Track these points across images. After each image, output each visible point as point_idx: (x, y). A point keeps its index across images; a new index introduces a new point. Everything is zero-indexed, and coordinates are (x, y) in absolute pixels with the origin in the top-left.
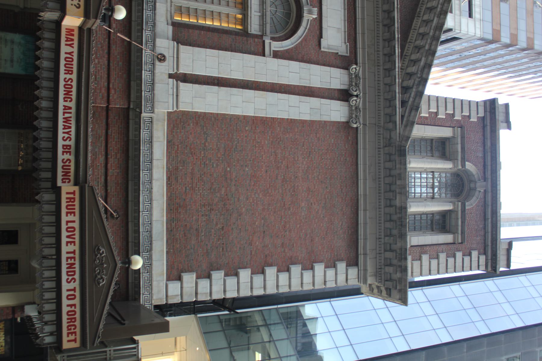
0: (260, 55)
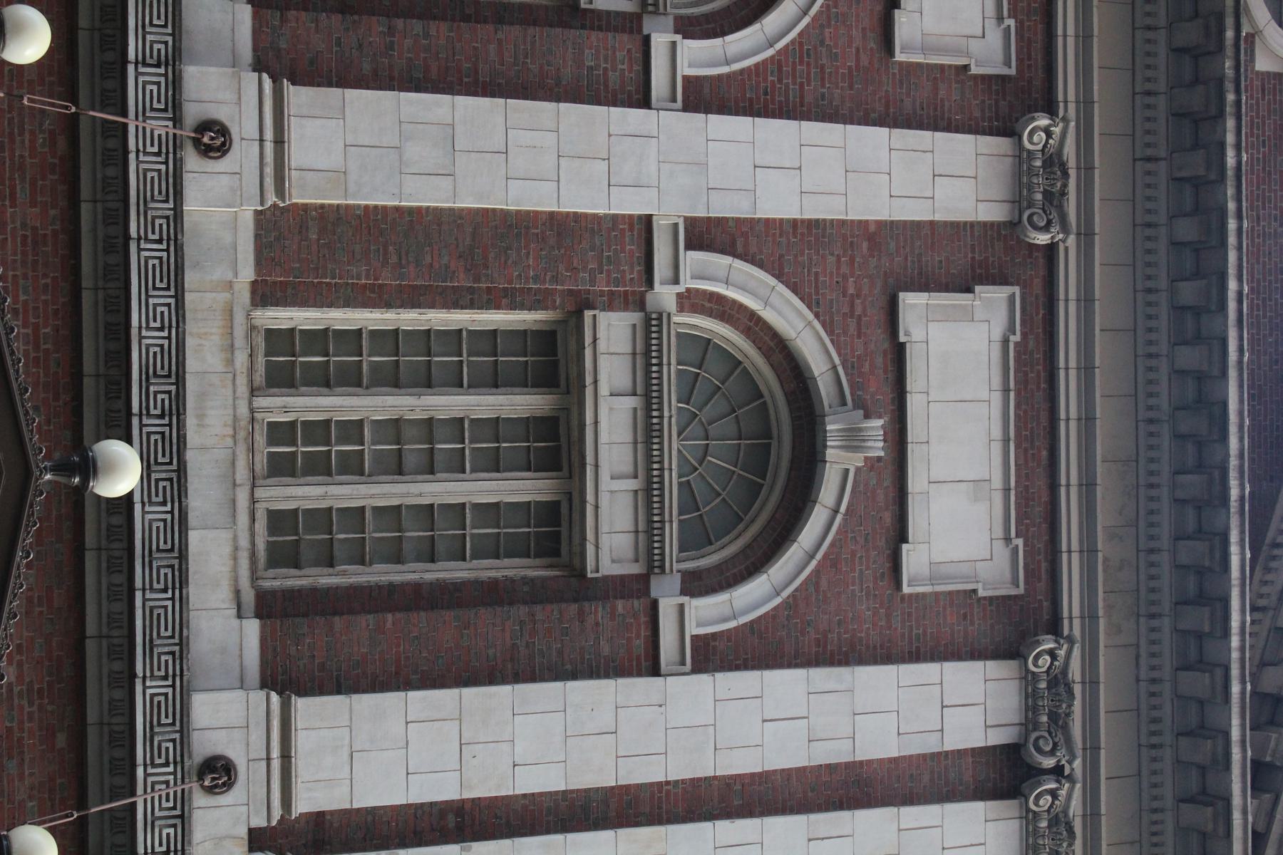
0: (640, 675)
